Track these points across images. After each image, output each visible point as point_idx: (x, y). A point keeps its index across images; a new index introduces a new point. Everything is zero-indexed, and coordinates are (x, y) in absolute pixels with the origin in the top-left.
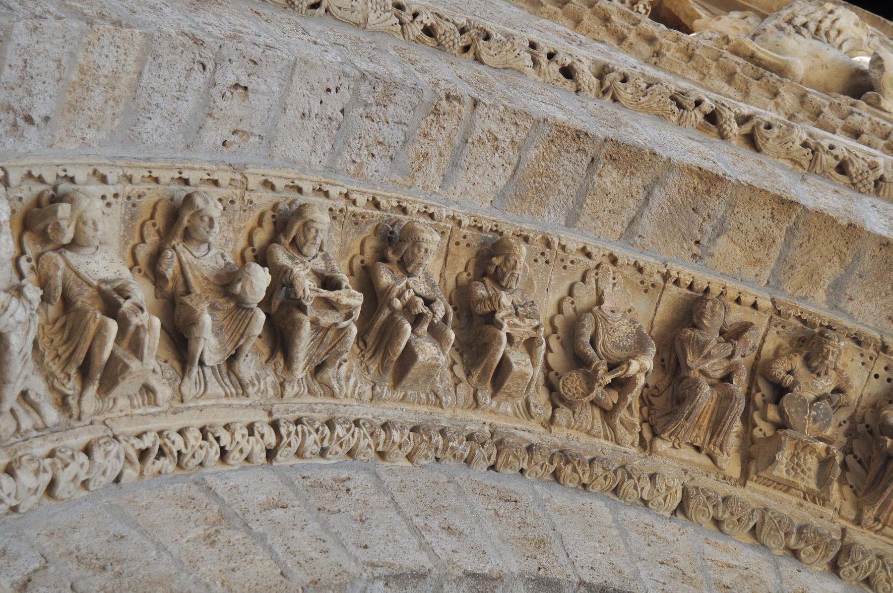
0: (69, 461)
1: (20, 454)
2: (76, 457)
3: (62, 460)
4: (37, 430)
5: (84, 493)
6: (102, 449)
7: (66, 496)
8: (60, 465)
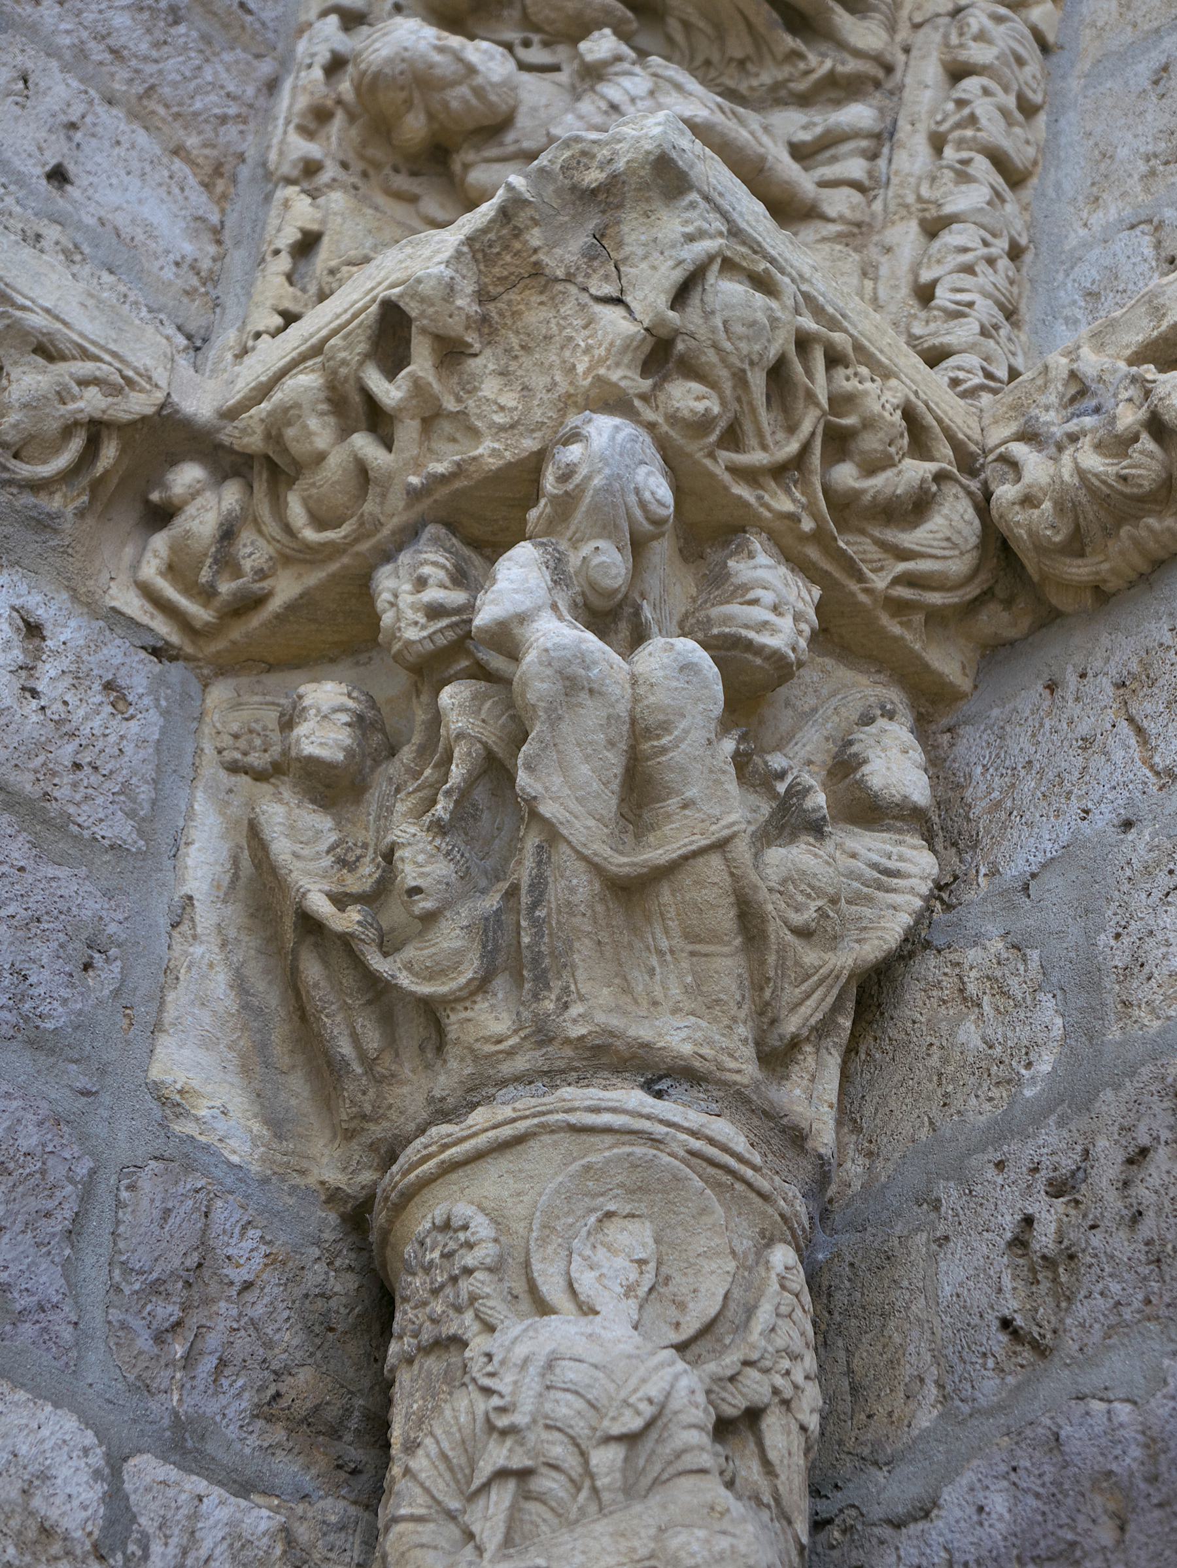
0: (966, 111)
1: (911, 199)
2: (964, 96)
3: (958, 125)
5: (1042, 118)
6: (972, 44)
7: (1031, 151)
8: (969, 133)
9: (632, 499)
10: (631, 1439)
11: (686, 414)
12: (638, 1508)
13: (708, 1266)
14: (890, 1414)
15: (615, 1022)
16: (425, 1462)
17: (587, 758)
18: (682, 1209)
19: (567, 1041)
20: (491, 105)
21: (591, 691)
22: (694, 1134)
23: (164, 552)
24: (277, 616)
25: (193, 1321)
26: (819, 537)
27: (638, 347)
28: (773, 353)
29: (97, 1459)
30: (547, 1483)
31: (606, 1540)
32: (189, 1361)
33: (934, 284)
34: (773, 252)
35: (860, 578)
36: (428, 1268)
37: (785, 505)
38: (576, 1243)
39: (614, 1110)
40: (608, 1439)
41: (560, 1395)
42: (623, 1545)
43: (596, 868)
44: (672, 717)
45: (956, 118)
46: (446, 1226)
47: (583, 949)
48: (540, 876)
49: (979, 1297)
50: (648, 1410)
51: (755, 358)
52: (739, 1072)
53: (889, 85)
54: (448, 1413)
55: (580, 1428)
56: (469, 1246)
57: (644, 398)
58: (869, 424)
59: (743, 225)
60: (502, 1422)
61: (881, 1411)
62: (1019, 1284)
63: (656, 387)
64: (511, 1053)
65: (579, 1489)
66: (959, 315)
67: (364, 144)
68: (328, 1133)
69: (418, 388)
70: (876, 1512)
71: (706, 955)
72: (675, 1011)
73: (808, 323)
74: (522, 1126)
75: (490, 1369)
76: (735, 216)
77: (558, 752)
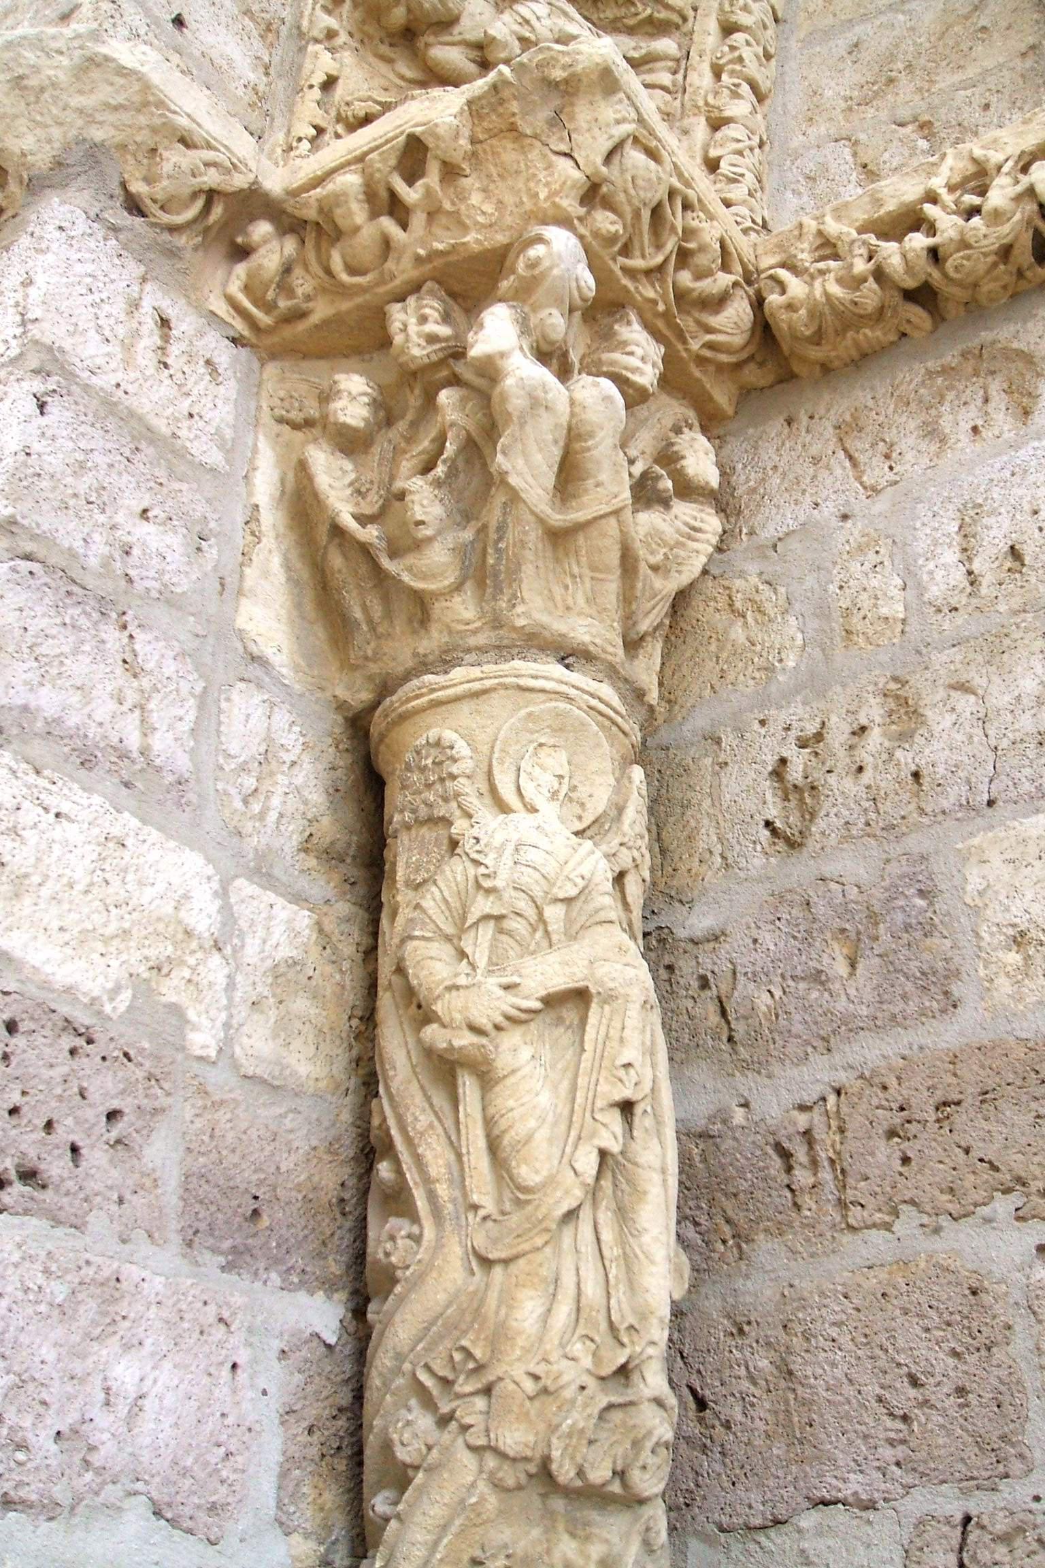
0: (736, 54)
1: (701, 103)
3: (731, 62)
4: (675, 73)
5: (773, 62)
7: (768, 83)
8: (738, 67)
10: (568, 901)
11: (604, 231)
12: (576, 947)
13: (598, 780)
14: (689, 871)
15: (544, 619)
16: (432, 903)
17: (540, 450)
19: (514, 628)
20: (449, 10)
22: (592, 695)
23: (243, 276)
24: (316, 326)
25: (263, 789)
26: (666, 315)
29: (215, 885)
30: (513, 924)
31: (557, 966)
32: (262, 816)
33: (718, 159)
35: (685, 342)
36: (423, 770)
37: (651, 294)
38: (523, 764)
40: (557, 900)
41: (524, 869)
42: (568, 970)
43: (541, 521)
45: (730, 57)
46: (438, 743)
47: (528, 570)
48: (505, 521)
49: (751, 805)
50: (581, 883)
53: (685, 29)
54: (448, 873)
55: (538, 893)
56: (455, 761)
58: (702, 248)
60: (487, 884)
61: (683, 868)
62: (777, 800)
64: (475, 632)
65: (535, 930)
66: (735, 181)
67: (364, 22)
68: (338, 664)
69: (429, 193)
70: (682, 933)
72: (580, 614)
74: (488, 683)
75: (478, 848)
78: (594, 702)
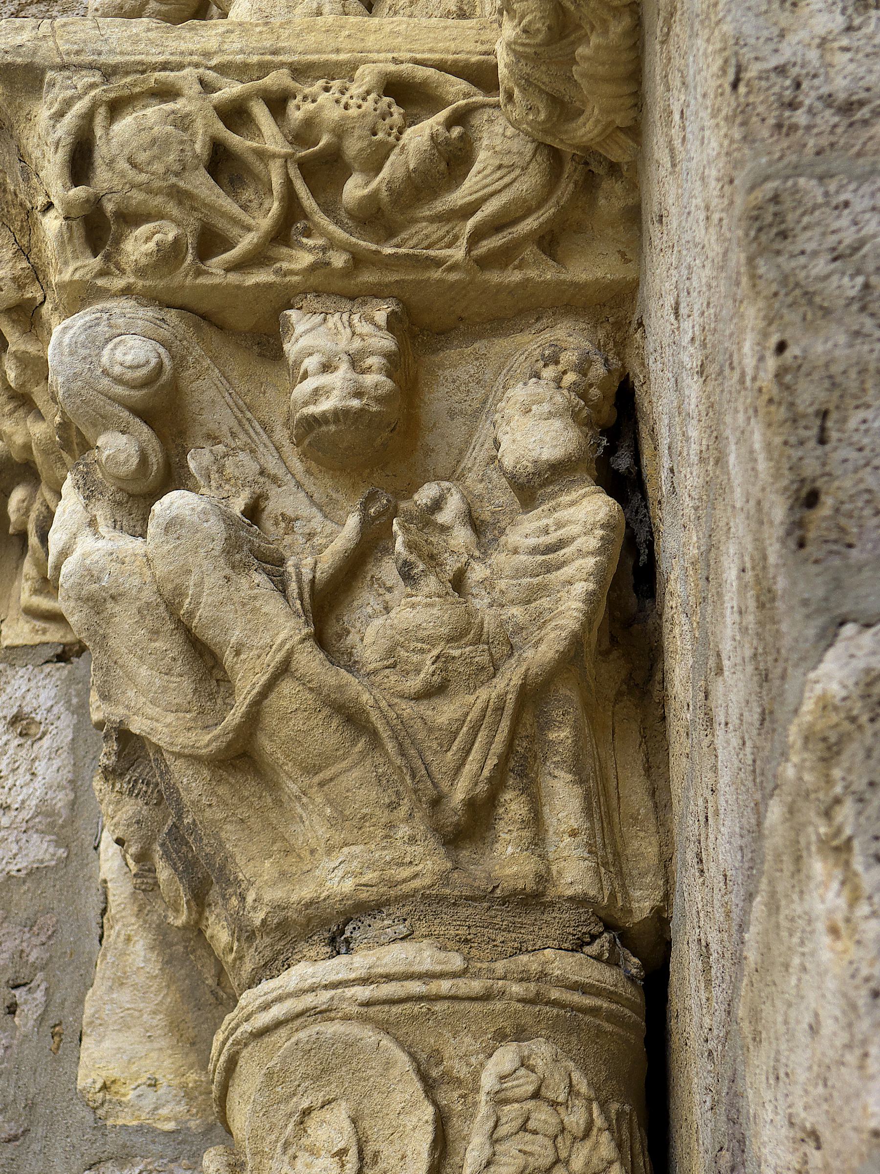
9: (105, 382)
11: (144, 261)
18: (370, 1072)
21: (113, 597)
26: (358, 260)
27: (70, 238)
28: (200, 146)
34: (161, 58)
35: (437, 263)
37: (305, 259)
39: (279, 999)
43: (194, 759)
44: (177, 581)
47: (230, 834)
51: (176, 167)
52: (416, 876)
57: (103, 273)
59: (119, 59)
63: (108, 258)
71: (331, 780)
72: (330, 850)
73: (231, 89)
76: (103, 59)
77: (121, 667)
78: (363, 993)
